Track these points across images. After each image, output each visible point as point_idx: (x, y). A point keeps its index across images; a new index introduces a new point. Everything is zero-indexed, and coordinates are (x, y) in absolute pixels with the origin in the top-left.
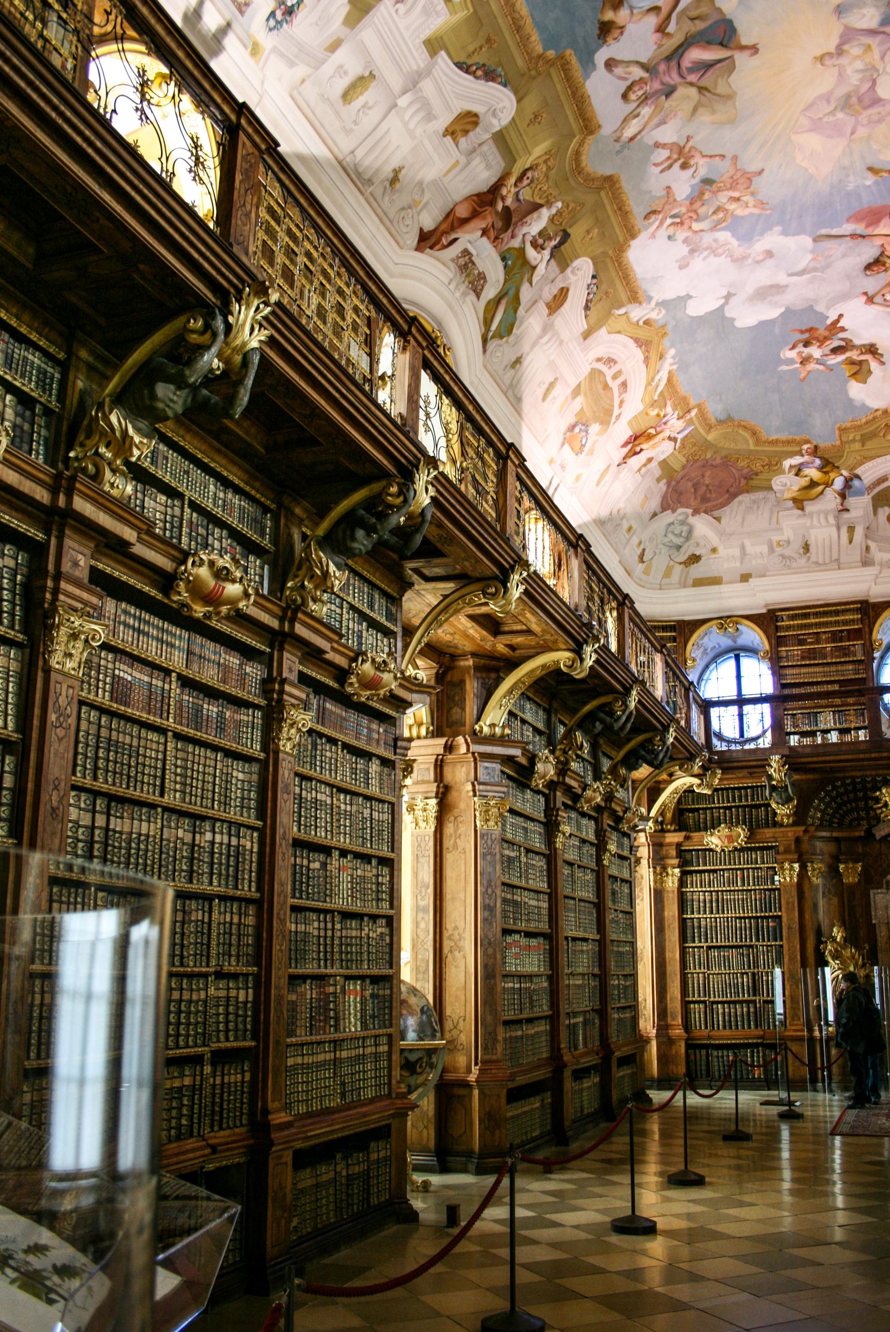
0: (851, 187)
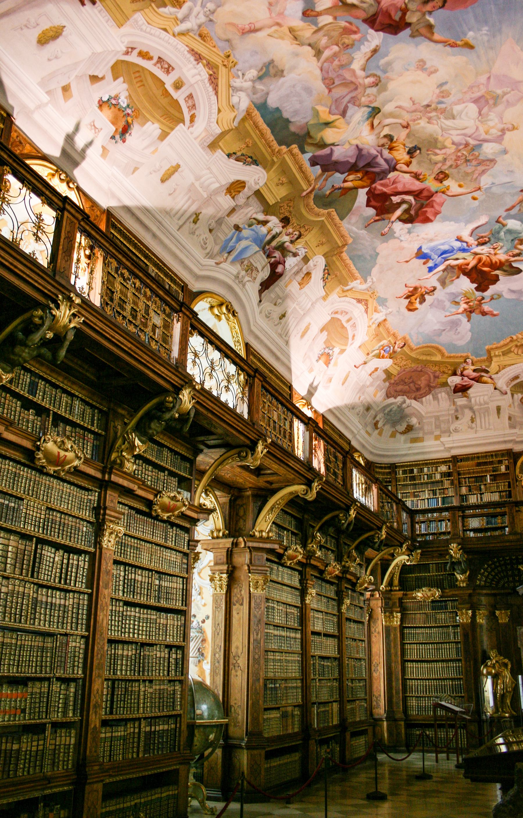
0: (485, 29)
